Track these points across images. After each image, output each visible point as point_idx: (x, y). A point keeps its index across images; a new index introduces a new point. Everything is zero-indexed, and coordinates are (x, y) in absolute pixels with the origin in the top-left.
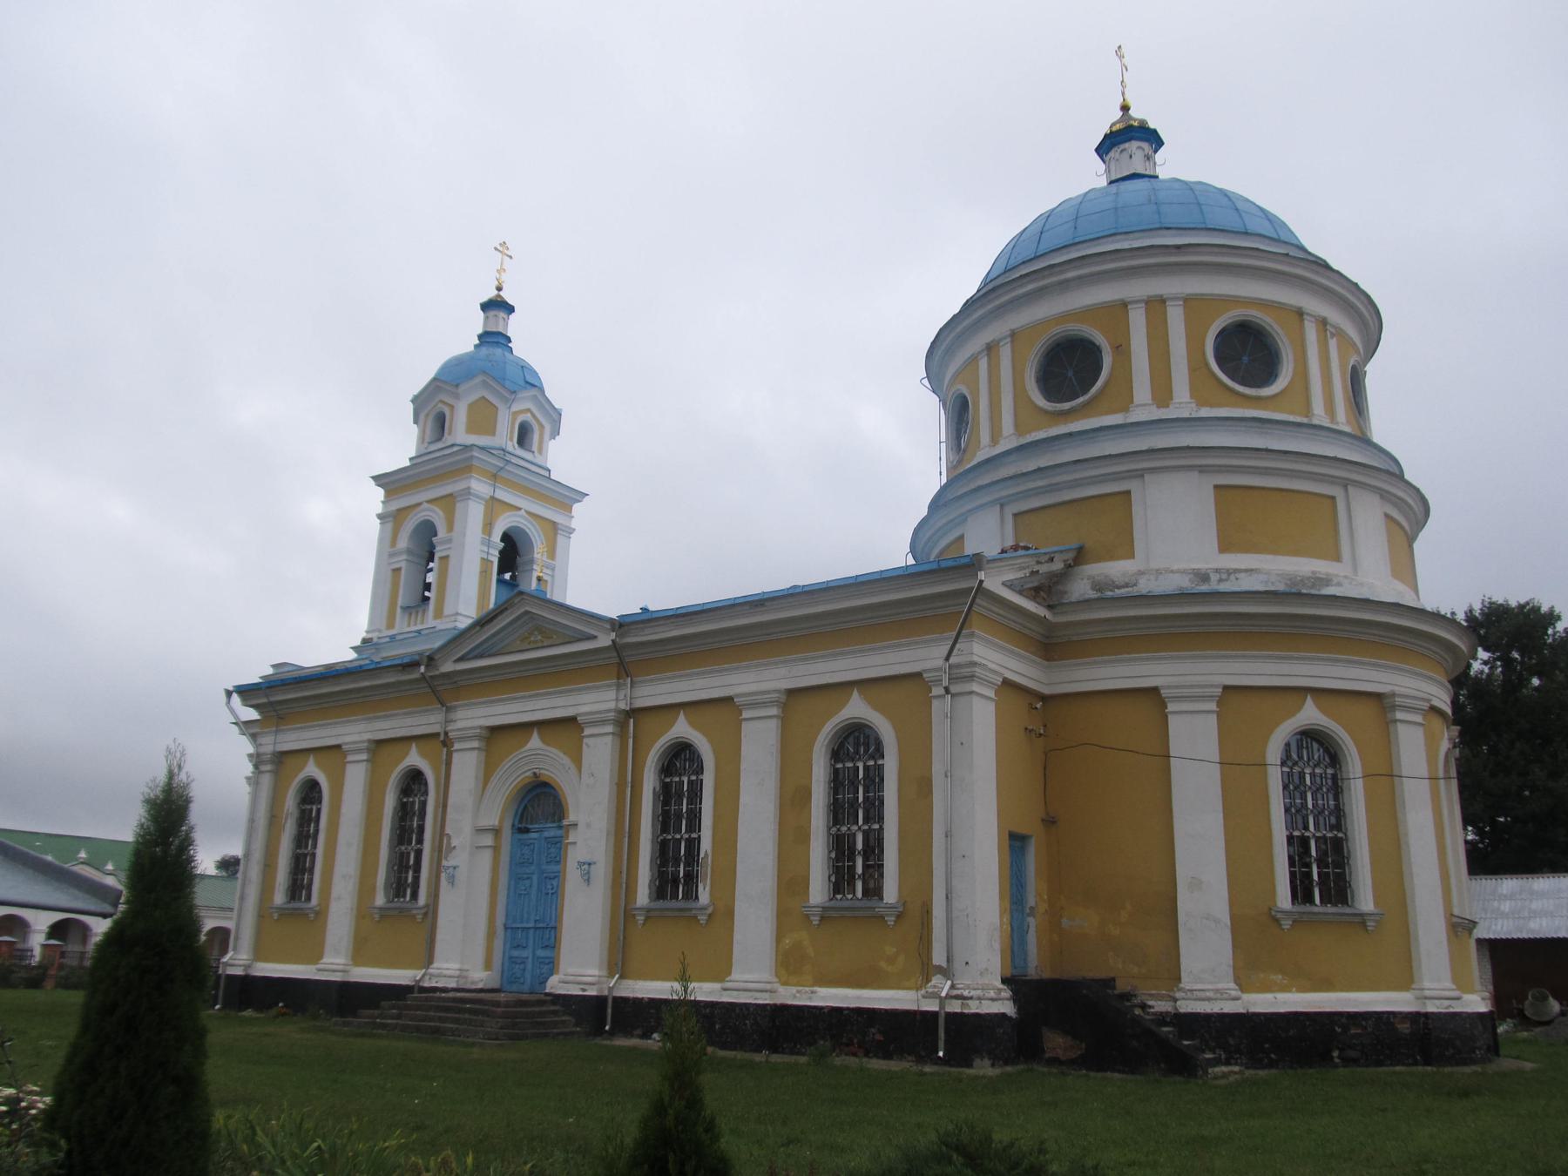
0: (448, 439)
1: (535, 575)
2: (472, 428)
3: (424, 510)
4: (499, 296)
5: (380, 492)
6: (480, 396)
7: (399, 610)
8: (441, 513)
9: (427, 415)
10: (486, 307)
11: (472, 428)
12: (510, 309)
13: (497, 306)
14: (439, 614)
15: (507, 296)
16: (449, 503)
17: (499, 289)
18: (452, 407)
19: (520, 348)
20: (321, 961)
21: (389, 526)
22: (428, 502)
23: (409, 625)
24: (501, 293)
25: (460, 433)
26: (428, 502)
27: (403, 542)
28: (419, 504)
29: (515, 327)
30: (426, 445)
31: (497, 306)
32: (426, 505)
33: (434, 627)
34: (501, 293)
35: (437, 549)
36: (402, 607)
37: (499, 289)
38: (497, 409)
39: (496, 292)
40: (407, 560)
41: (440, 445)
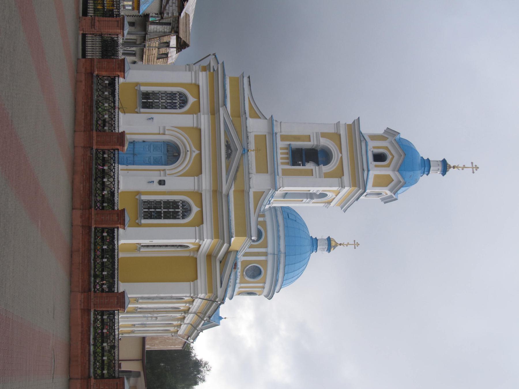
2: (376, 177)
3: (337, 153)
4: (450, 167)
5: (350, 122)
6: (394, 179)
7: (288, 143)
8: (335, 167)
9: (387, 148)
10: (444, 162)
11: (376, 177)
12: (444, 172)
13: (445, 167)
14: (286, 173)
15: (451, 171)
18: (388, 166)
19: (424, 179)
21: (332, 130)
22: (342, 157)
23: (281, 149)
24: (452, 168)
26: (342, 157)
27: (324, 142)
28: (341, 153)
29: (435, 175)
30: (372, 149)
31: (445, 167)
32: (340, 155)
33: (278, 175)
34: (452, 168)
36: (290, 145)
37: (454, 167)
38: (387, 186)
39: (452, 166)
40: (314, 145)
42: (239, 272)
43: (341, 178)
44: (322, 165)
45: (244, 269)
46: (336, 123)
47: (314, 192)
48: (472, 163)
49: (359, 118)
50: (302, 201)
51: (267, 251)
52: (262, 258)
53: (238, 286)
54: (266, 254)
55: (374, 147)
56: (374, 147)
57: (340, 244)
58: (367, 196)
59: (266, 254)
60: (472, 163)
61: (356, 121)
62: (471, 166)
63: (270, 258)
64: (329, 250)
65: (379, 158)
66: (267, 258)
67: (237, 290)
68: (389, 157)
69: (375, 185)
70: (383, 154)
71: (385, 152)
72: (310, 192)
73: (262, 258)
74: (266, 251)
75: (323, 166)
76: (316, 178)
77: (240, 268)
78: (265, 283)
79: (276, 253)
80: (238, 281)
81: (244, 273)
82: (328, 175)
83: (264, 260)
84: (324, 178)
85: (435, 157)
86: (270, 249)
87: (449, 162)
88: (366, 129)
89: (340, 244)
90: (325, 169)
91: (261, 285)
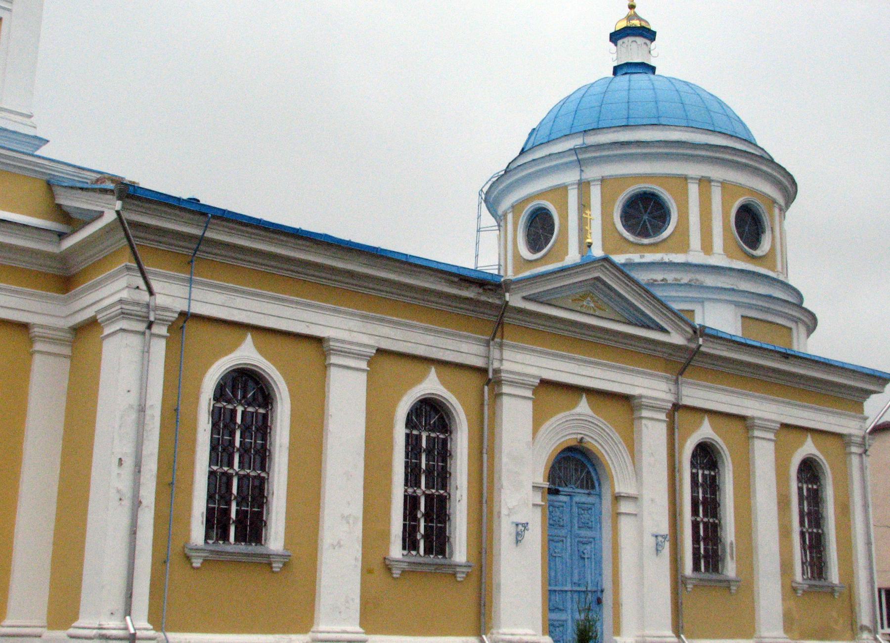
20: (76, 624)
42: (642, 257)
45: (632, 243)
51: (574, 184)
52: (595, 193)
53: (696, 257)
54: (583, 186)
57: (632, 7)
59: (583, 186)
63: (593, 173)
64: (648, 34)
66: (594, 181)
67: (718, 259)
73: (595, 193)
74: (576, 186)
77: (628, 256)
78: (685, 178)
79: (575, 158)
80: (678, 258)
81: (646, 241)
83: (602, 188)
86: (571, 177)
89: (632, 7)
91: (693, 189)
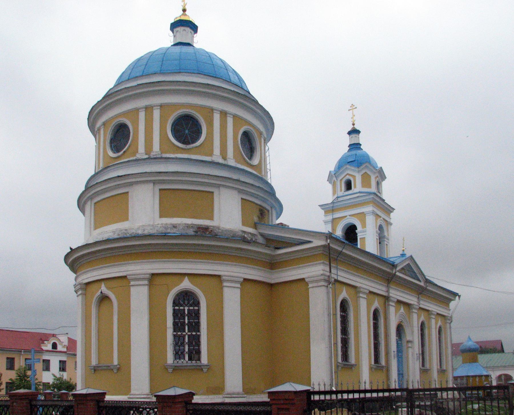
0: (354, 190)
1: (386, 243)
3: (347, 219)
4: (354, 127)
5: (323, 212)
6: (365, 172)
10: (350, 133)
11: (363, 186)
13: (354, 132)
15: (357, 127)
16: (362, 216)
17: (354, 125)
24: (355, 126)
25: (358, 187)
28: (346, 216)
31: (354, 132)
34: (355, 126)
35: (358, 235)
37: (354, 125)
39: (353, 126)
41: (350, 192)
43: (365, 214)
44: (356, 231)
46: (324, 223)
47: (378, 235)
48: (349, 110)
49: (319, 206)
50: (387, 245)
55: (341, 190)
56: (341, 191)
58: (380, 192)
60: (349, 110)
61: (323, 208)
62: (351, 111)
65: (349, 186)
68: (348, 177)
69: (369, 186)
70: (346, 182)
71: (344, 181)
72: (378, 238)
75: (357, 229)
76: (366, 234)
82: (364, 225)
84: (366, 228)
85: (346, 141)
87: (350, 128)
88: (329, 199)
90: (359, 229)
